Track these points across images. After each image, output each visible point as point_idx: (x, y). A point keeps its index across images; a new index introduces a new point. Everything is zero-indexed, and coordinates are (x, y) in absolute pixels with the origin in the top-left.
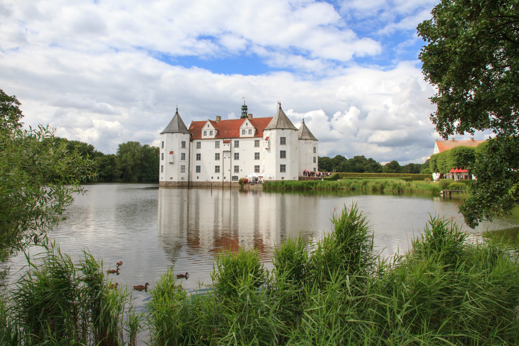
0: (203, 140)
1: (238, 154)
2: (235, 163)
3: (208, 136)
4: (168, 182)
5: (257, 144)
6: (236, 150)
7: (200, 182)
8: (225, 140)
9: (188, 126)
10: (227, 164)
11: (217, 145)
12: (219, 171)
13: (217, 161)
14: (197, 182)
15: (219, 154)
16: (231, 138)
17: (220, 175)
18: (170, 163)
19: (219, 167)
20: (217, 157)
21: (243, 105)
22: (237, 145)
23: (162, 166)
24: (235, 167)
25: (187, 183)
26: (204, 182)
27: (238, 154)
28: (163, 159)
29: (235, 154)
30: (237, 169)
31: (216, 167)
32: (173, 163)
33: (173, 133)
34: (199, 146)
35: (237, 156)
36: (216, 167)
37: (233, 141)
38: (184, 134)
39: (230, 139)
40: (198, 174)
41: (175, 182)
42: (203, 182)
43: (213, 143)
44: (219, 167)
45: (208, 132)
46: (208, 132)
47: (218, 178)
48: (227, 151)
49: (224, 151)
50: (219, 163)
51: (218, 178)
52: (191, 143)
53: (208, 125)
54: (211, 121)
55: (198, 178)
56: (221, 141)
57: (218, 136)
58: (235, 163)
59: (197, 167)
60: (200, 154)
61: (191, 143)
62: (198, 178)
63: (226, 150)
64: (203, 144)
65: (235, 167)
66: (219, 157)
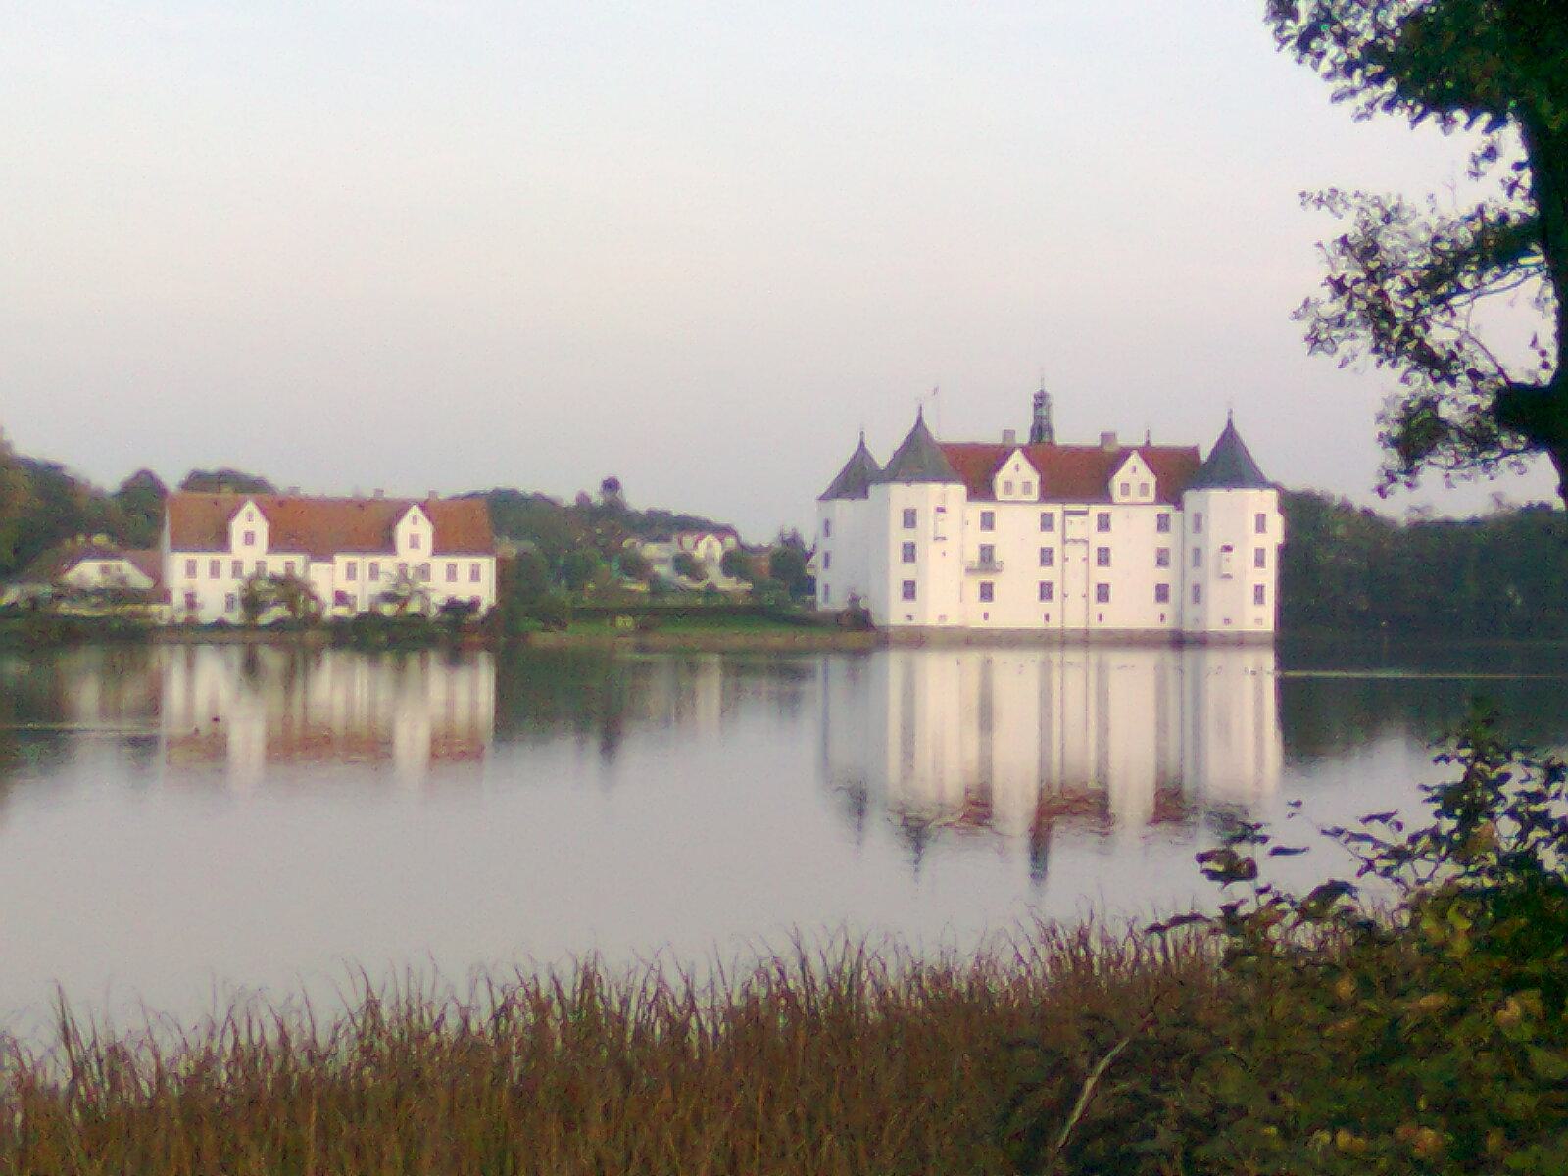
0: (1004, 506)
1: (1107, 550)
2: (1101, 575)
5: (1163, 524)
6: (1101, 539)
10: (1075, 575)
11: (1047, 523)
13: (1047, 569)
15: (1051, 551)
17: (1052, 607)
19: (1050, 585)
20: (1046, 557)
21: (1037, 390)
22: (1104, 524)
27: (1107, 550)
30: (1103, 593)
34: (987, 522)
35: (1104, 557)
37: (1095, 510)
39: (1082, 507)
40: (986, 606)
44: (1050, 585)
47: (1047, 618)
48: (1075, 541)
51: (1047, 618)
55: (986, 616)
56: (1056, 509)
57: (1048, 494)
58: (1101, 575)
62: (986, 616)
64: (1003, 515)
65: (1099, 586)
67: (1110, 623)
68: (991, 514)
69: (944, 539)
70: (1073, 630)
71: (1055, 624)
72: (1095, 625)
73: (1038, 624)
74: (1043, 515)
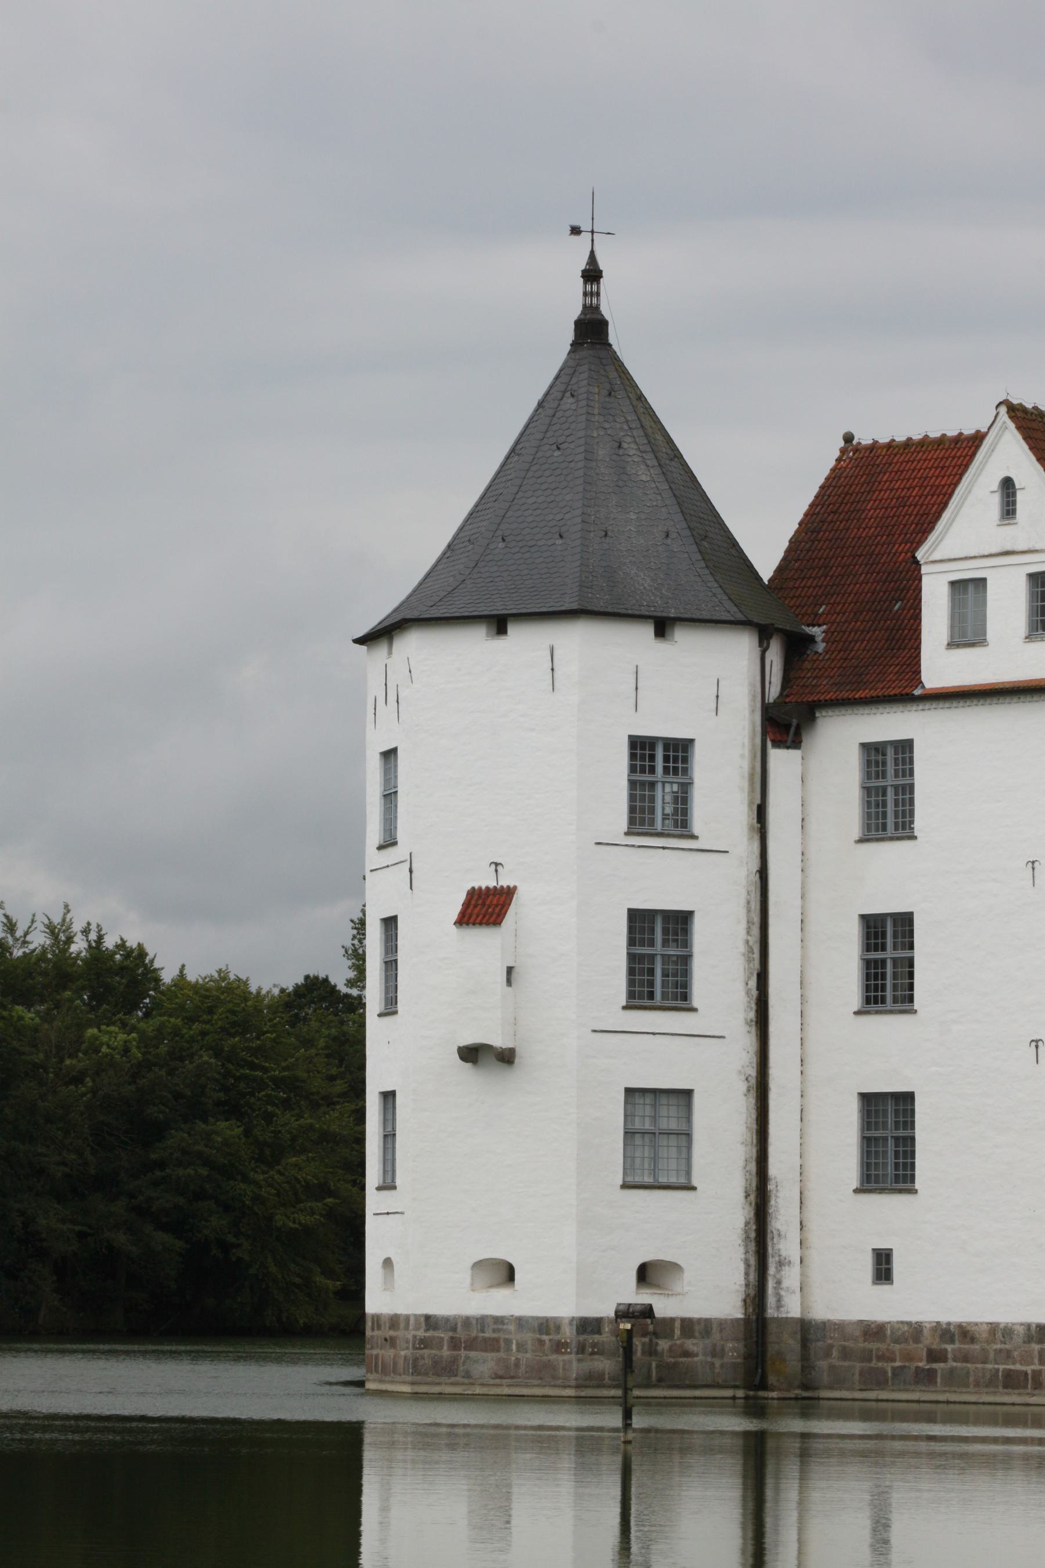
4: (450, 1324)
7: (916, 1330)
14: (874, 1331)
18: (471, 1054)
23: (389, 1097)
25: (734, 1350)
26: (964, 1333)
28: (390, 1008)
32: (506, 1057)
33: (500, 625)
38: (662, 628)
41: (546, 1326)
42: (947, 1332)
52: (777, 756)
53: (1008, 486)
59: (871, 1102)
60: (904, 922)
61: (780, 759)
68: (905, 747)
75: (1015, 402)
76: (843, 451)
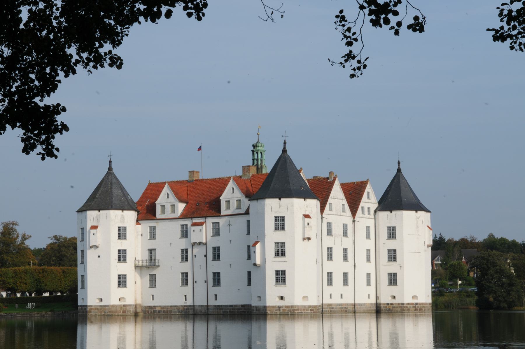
2: (215, 267)
3: (168, 214)
6: (213, 242)
8: (195, 221)
9: (136, 195)
12: (187, 284)
16: (206, 217)
17: (188, 290)
19: (187, 274)
21: (255, 142)
24: (214, 274)
29: (214, 248)
30: (217, 279)
31: (183, 274)
35: (217, 254)
36: (183, 274)
37: (210, 221)
40: (153, 291)
43: (176, 227)
44: (187, 274)
45: (168, 208)
46: (168, 208)
48: (200, 243)
49: (194, 244)
50: (186, 267)
54: (174, 185)
63: (198, 242)
65: (214, 274)
66: (187, 256)
67: (223, 301)
68: (155, 227)
69: (97, 247)
70: (199, 306)
71: (189, 302)
72: (212, 302)
73: (180, 302)
74: (182, 225)
75: (169, 181)
76: (149, 184)
